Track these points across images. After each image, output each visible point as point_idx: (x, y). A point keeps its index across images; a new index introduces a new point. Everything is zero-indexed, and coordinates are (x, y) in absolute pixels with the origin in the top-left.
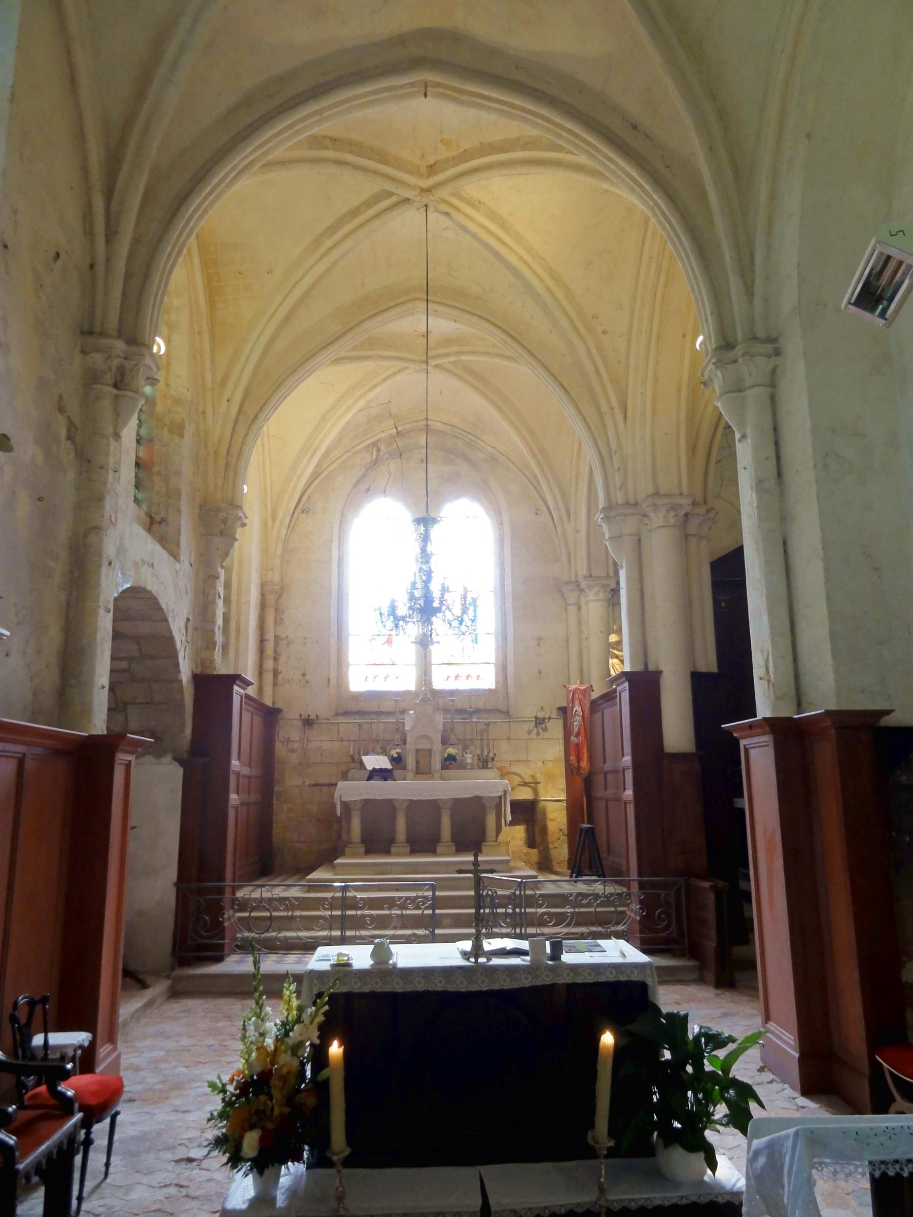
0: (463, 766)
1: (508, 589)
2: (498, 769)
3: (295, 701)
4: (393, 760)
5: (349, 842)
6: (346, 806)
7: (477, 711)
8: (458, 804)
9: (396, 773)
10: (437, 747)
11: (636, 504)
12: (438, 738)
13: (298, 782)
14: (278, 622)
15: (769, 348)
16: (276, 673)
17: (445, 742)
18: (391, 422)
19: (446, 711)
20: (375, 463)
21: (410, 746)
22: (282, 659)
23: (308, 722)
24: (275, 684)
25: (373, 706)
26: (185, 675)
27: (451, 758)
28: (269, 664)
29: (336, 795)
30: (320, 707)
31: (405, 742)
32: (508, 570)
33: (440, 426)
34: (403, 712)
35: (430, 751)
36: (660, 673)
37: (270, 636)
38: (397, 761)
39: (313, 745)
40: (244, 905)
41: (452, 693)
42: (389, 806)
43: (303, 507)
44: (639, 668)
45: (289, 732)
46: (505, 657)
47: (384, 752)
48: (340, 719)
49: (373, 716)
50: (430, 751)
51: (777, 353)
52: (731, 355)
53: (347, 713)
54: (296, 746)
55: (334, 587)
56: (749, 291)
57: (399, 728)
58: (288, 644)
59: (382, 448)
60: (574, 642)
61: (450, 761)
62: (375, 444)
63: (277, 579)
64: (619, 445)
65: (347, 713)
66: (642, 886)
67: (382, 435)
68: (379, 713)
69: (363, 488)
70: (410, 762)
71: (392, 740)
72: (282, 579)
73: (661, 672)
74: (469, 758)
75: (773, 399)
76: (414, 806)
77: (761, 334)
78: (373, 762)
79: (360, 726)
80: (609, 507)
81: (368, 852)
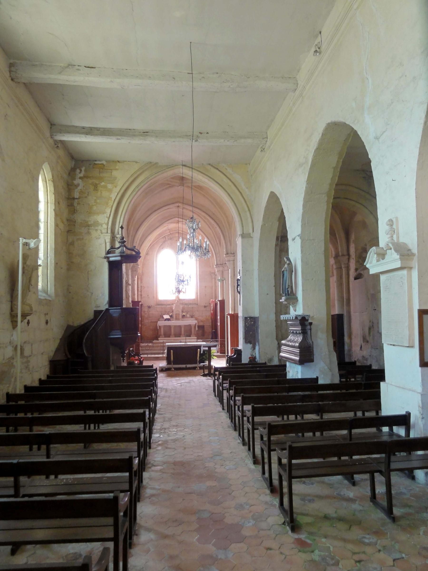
0: (187, 317)
2: (195, 318)
3: (146, 302)
4: (170, 316)
5: (161, 335)
6: (160, 327)
7: (190, 304)
9: (171, 319)
10: (181, 313)
11: (222, 264)
13: (147, 321)
14: (141, 282)
15: (233, 255)
16: (141, 295)
17: (182, 312)
18: (168, 231)
19: (182, 304)
20: (164, 242)
21: (174, 313)
22: (142, 292)
23: (149, 307)
24: (141, 298)
26: (130, 301)
27: (184, 316)
28: (140, 293)
30: (152, 303)
34: (173, 304)
35: (179, 314)
38: (171, 316)
39: (151, 312)
40: (142, 347)
41: (184, 300)
42: (170, 327)
43: (147, 254)
44: (222, 299)
45: (145, 309)
47: (168, 314)
48: (158, 306)
49: (166, 306)
50: (179, 314)
52: (227, 255)
53: (158, 305)
54: (146, 313)
55: (155, 274)
56: (231, 245)
57: (171, 308)
58: (144, 288)
60: (214, 288)
63: (141, 272)
64: (219, 252)
65: (158, 305)
66: (220, 341)
68: (166, 305)
69: (162, 247)
71: (170, 311)
72: (142, 272)
74: (188, 316)
75: (234, 263)
76: (175, 326)
78: (166, 317)
80: (217, 265)
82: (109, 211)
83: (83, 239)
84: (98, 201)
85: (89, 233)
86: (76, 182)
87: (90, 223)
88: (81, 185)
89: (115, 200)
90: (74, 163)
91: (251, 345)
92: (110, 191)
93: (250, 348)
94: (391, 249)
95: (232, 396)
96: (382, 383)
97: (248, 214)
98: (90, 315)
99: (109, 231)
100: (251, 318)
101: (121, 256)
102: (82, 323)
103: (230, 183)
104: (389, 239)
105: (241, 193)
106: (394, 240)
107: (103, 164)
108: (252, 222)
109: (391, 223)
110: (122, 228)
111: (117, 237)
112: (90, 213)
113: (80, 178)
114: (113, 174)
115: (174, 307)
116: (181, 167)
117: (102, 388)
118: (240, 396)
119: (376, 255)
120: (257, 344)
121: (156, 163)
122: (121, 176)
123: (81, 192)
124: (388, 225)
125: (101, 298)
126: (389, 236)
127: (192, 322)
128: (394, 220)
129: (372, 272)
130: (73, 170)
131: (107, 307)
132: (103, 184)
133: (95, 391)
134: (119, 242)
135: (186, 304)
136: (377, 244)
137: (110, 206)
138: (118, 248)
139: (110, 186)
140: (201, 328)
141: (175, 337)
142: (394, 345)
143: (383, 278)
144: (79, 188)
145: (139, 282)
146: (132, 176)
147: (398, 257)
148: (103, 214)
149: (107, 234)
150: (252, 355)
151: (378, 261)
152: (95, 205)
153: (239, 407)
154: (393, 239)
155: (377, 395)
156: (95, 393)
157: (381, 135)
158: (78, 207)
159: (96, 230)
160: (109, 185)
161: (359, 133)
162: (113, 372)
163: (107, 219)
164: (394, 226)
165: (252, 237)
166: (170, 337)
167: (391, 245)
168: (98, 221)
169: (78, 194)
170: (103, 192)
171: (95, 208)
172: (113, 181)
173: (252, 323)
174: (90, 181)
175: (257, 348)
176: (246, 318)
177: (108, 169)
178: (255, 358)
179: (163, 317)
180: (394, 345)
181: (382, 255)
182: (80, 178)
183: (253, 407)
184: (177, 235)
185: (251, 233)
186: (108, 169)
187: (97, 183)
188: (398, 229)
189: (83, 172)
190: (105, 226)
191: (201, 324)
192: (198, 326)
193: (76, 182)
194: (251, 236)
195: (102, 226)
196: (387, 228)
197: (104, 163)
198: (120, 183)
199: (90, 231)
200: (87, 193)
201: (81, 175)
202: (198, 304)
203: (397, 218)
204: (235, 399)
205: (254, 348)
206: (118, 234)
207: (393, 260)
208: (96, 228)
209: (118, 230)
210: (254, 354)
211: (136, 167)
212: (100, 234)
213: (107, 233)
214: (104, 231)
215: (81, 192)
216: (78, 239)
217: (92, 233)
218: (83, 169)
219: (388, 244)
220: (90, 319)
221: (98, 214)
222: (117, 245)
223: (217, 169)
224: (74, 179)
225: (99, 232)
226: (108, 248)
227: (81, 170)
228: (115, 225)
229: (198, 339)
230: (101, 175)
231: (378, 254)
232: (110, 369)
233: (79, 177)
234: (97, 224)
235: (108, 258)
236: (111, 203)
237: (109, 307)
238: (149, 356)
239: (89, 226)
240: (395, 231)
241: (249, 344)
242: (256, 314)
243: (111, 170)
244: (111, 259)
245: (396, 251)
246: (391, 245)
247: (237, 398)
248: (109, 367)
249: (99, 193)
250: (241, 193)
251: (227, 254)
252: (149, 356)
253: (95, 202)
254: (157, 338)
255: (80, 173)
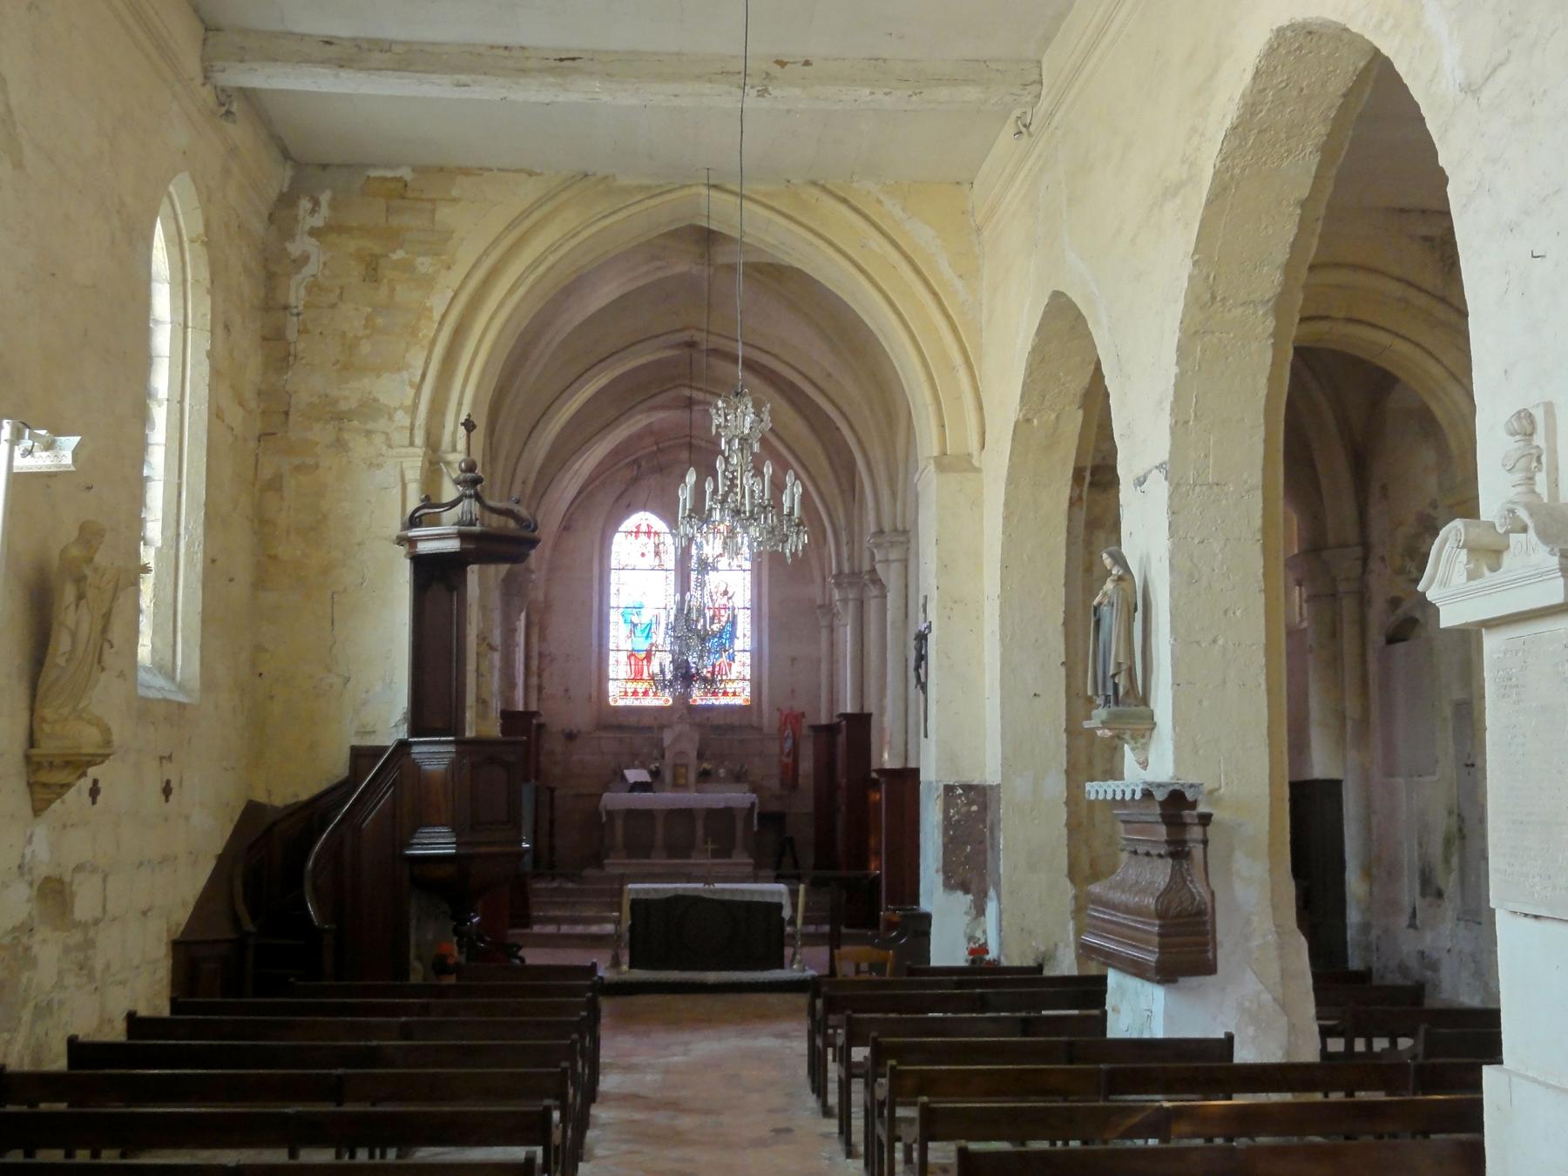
0: (718, 780)
1: (765, 608)
6: (610, 814)
8: (712, 814)
12: (693, 754)
14: (542, 638)
15: (902, 539)
16: (540, 688)
17: (700, 756)
20: (635, 480)
22: (546, 675)
23: (570, 736)
25: (633, 720)
28: (534, 680)
29: (602, 804)
30: (581, 719)
31: (663, 756)
32: (765, 590)
33: (703, 444)
34: (662, 727)
36: (869, 716)
37: (535, 654)
38: (656, 774)
42: (648, 814)
43: (567, 527)
44: (857, 710)
46: (760, 677)
47: (643, 766)
51: (908, 541)
55: (596, 604)
56: (894, 494)
57: (659, 745)
59: (643, 463)
61: (705, 776)
62: (635, 461)
63: (541, 597)
65: (607, 727)
67: (641, 453)
70: (668, 776)
72: (546, 596)
73: (869, 716)
74: (722, 772)
77: (900, 527)
78: (633, 775)
79: (621, 740)
81: (629, 856)
82: (420, 361)
83: (317, 466)
84: (380, 321)
85: (340, 445)
86: (294, 249)
87: (343, 406)
88: (313, 259)
89: (444, 317)
90: (289, 173)
91: (970, 897)
92: (427, 283)
93: (965, 908)
94: (1524, 529)
95: (882, 1104)
96: (1487, 1071)
97: (962, 374)
98: (338, 767)
99: (419, 439)
100: (968, 788)
101: (462, 536)
102: (304, 796)
103: (894, 256)
104: (1519, 489)
105: (935, 294)
106: (1539, 496)
107: (399, 179)
108: (980, 408)
109: (1524, 425)
110: (469, 425)
111: (448, 464)
112: (348, 367)
113: (313, 232)
114: (439, 215)
115: (668, 738)
116: (704, 191)
117: (372, 1057)
118: (915, 1104)
119: (1464, 552)
120: (992, 893)
121: (606, 177)
122: (472, 228)
123: (314, 287)
124: (1513, 434)
125: (382, 703)
126: (1518, 476)
127: (738, 797)
128: (1539, 415)
129: (1448, 619)
130: (287, 200)
131: (402, 733)
132: (399, 255)
133: (340, 1071)
134: (457, 482)
135: (716, 728)
136: (1467, 507)
137: (426, 342)
138: (453, 504)
139: (424, 264)
140: (772, 820)
141: (670, 857)
142: (1536, 917)
143: (1492, 643)
144: (310, 269)
145: (535, 639)
146: (511, 226)
147: (1554, 561)
148: (399, 370)
149: (411, 450)
150: (971, 938)
151: (1472, 576)
152: (368, 337)
153: (908, 1151)
154: (1533, 492)
155: (1470, 1117)
156: (339, 1077)
157: (1488, 79)
158: (301, 346)
159: (369, 433)
160: (420, 260)
161: (1401, 67)
162: (418, 991)
163: (411, 392)
164: (1539, 439)
165: (978, 470)
166: (648, 857)
167: (1523, 514)
168: (375, 400)
169: (302, 292)
170: (398, 288)
171: (365, 348)
172: (439, 242)
173: (974, 808)
174: (352, 245)
175: (992, 908)
176: (949, 789)
177: (418, 199)
178: (983, 949)
179: (623, 778)
180: (1536, 917)
181: (1489, 554)
182: (313, 232)
183: (963, 1153)
184: (684, 455)
185: (975, 454)
186: (418, 199)
187: (377, 250)
188: (1553, 451)
189: (324, 210)
190: (402, 418)
191: (774, 807)
192: (762, 816)
193: (294, 249)
194: (975, 462)
195: (391, 418)
196: (1512, 444)
197: (406, 173)
198: (466, 255)
199: (346, 436)
200: (337, 291)
201: (318, 221)
202: (759, 729)
203: (1549, 408)
204: (892, 1112)
205: (981, 911)
206: (454, 450)
207: (1532, 575)
208: (370, 426)
209: (455, 433)
210: (978, 934)
211: (529, 191)
212: (384, 449)
213: (412, 444)
214: (401, 438)
215: (314, 287)
216: (298, 469)
217: (351, 445)
218: (325, 198)
219: (1512, 511)
220: (336, 781)
221: (378, 371)
222: (449, 492)
223: (844, 201)
224: (288, 234)
225: (379, 440)
226: (413, 502)
227: (316, 204)
228: (444, 414)
229: (758, 866)
230: (395, 221)
231: (1473, 550)
232: (407, 978)
233: (307, 228)
234: (370, 409)
235: (412, 542)
236: (427, 331)
237: (416, 729)
238: (565, 929)
239: (340, 417)
240: (1544, 459)
241: (960, 893)
242: (990, 773)
243: (433, 201)
244: (424, 547)
245: (1545, 536)
246: (1523, 514)
247: (901, 1112)
248: (402, 971)
249: (384, 290)
250: (935, 294)
251: (881, 532)
252: (565, 929)
253: (366, 327)
254: (597, 860)
255: (313, 211)
